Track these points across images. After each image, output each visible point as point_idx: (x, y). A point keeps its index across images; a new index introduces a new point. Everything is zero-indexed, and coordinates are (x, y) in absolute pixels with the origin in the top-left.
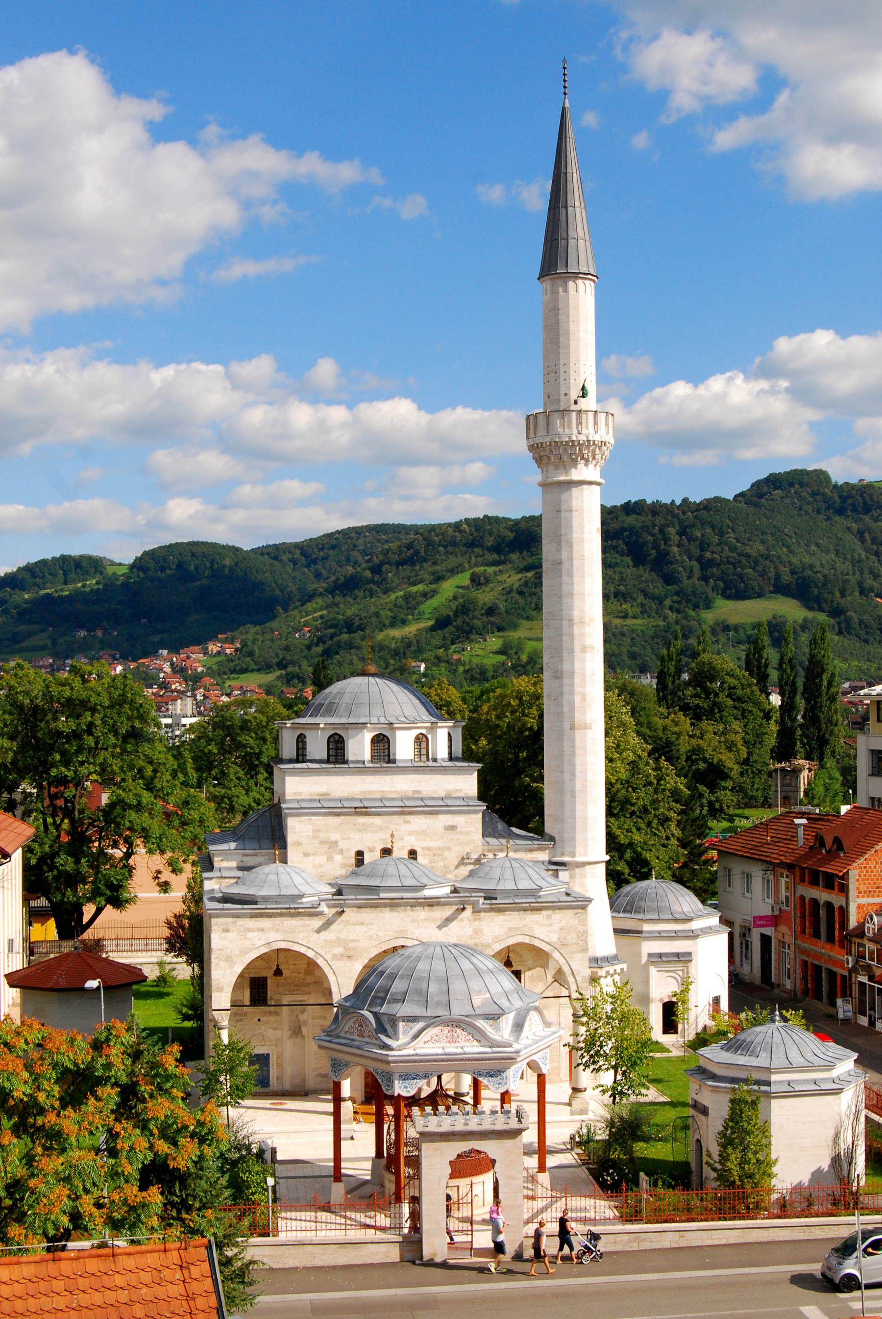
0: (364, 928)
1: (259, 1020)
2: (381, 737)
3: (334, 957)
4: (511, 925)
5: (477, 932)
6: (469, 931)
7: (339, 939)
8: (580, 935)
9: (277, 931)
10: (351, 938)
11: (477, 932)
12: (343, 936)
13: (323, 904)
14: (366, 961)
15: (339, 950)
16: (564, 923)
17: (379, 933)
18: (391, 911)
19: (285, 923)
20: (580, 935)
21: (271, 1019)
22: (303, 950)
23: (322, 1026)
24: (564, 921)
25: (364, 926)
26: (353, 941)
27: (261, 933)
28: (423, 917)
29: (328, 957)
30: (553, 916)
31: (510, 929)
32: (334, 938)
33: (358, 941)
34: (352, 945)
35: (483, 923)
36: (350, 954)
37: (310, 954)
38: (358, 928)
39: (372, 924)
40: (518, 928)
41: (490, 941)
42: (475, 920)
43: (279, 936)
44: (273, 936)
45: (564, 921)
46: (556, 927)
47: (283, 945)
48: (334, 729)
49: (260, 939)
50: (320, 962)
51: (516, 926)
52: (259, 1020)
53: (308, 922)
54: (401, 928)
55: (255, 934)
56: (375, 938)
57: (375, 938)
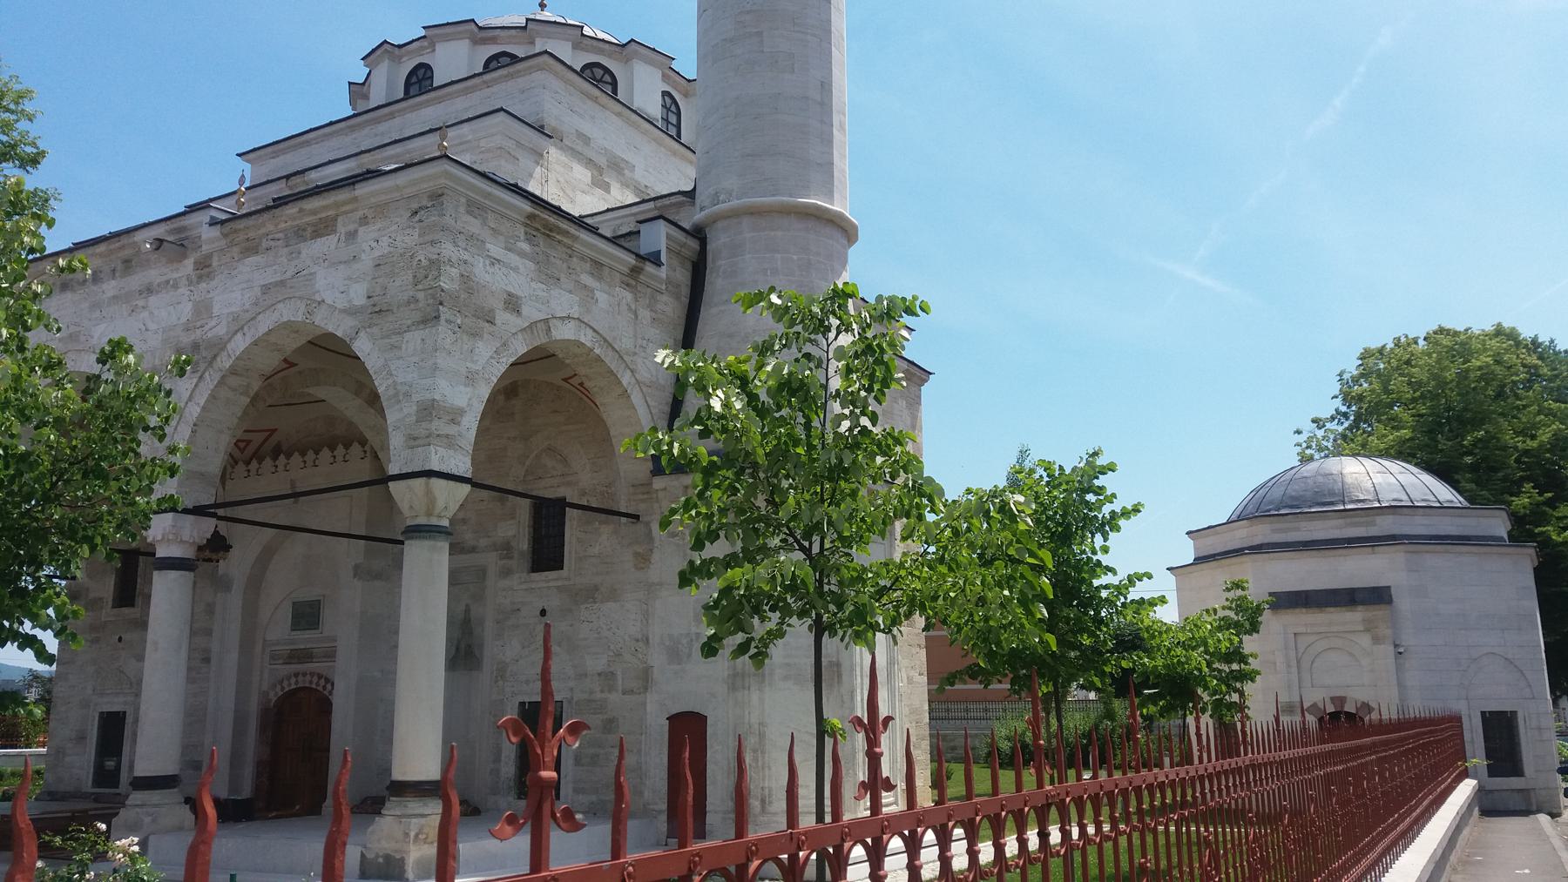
1: (120, 639)
4: (270, 277)
5: (203, 309)
6: (186, 310)
8: (420, 276)
11: (203, 309)
16: (384, 247)
20: (420, 276)
24: (385, 241)
28: (110, 294)
30: (361, 230)
31: (266, 289)
35: (213, 283)
40: (282, 283)
41: (221, 330)
42: (200, 278)
45: (385, 241)
46: (367, 261)
51: (278, 278)
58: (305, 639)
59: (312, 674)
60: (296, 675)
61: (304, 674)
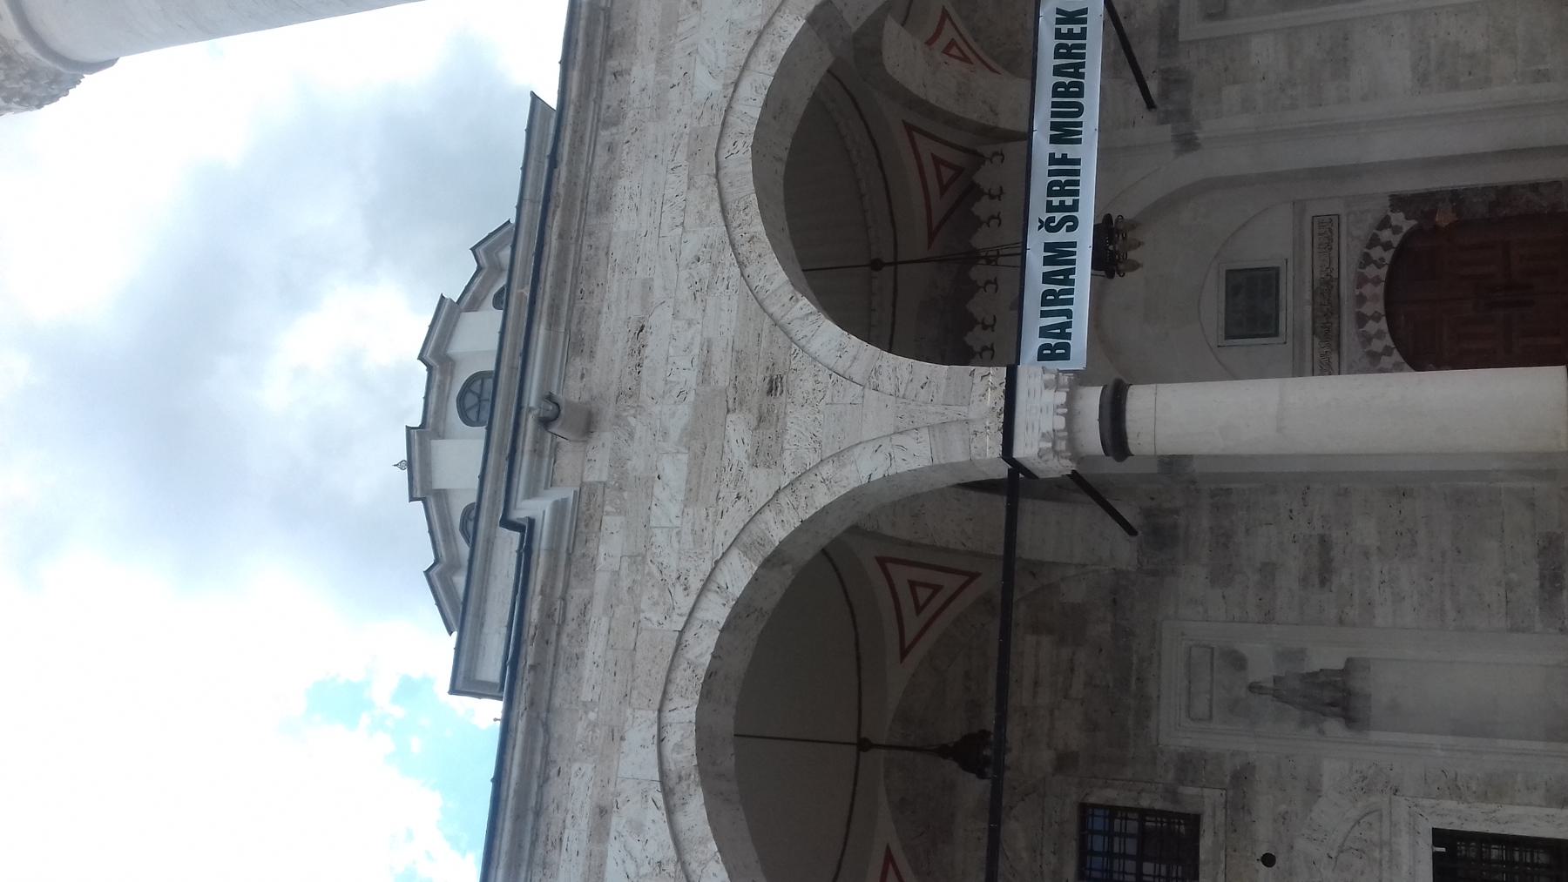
0: (661, 320)
1: (1268, 860)
2: (471, 400)
3: (764, 456)
7: (691, 433)
9: (616, 736)
10: (691, 377)
12: (679, 418)
13: (524, 509)
14: (805, 305)
15: (738, 432)
17: (688, 252)
18: (604, 206)
19: (587, 694)
21: (1265, 805)
22: (717, 611)
23: (1304, 581)
25: (653, 321)
26: (706, 367)
27: (617, 823)
29: (761, 483)
32: (684, 458)
33: (708, 346)
34: (722, 374)
36: (758, 379)
37: (738, 575)
38: (656, 347)
39: (647, 286)
43: (640, 732)
44: (637, 761)
47: (684, 712)
48: (447, 532)
49: (637, 828)
50: (778, 530)
52: (1268, 860)
53: (602, 581)
54: (681, 158)
55: (614, 849)
56: (704, 268)
57: (704, 268)
58: (1295, 306)
59: (1362, 281)
60: (1361, 320)
61: (1361, 299)
